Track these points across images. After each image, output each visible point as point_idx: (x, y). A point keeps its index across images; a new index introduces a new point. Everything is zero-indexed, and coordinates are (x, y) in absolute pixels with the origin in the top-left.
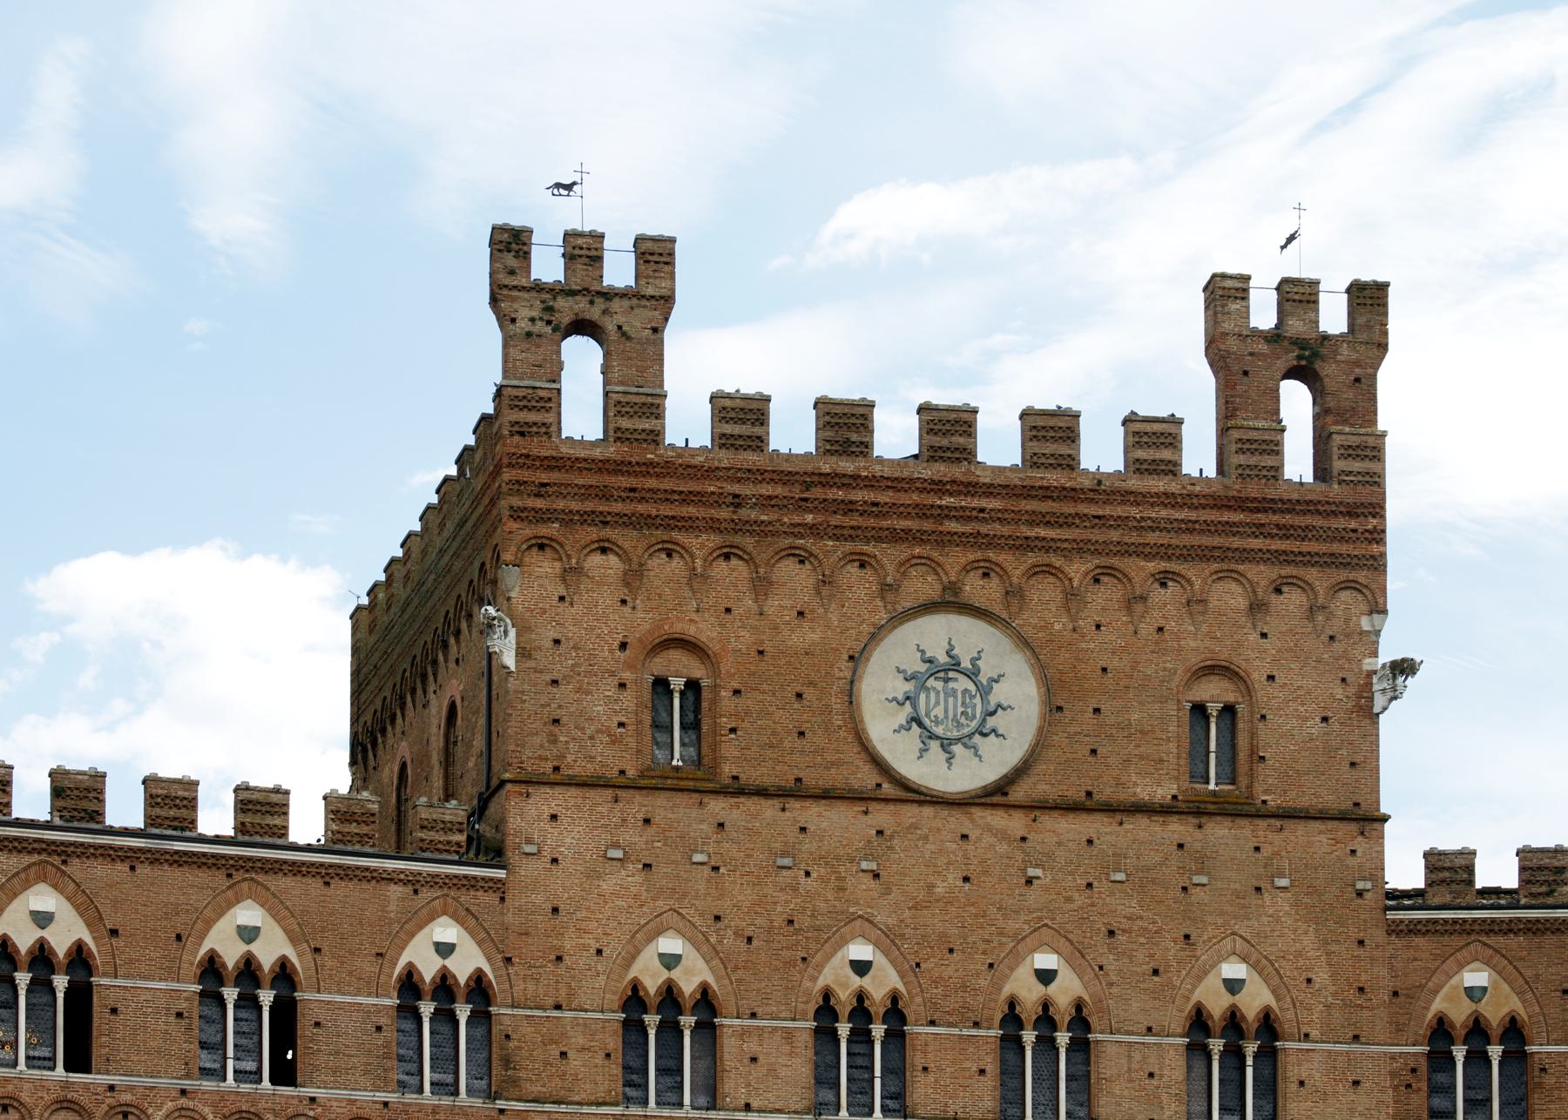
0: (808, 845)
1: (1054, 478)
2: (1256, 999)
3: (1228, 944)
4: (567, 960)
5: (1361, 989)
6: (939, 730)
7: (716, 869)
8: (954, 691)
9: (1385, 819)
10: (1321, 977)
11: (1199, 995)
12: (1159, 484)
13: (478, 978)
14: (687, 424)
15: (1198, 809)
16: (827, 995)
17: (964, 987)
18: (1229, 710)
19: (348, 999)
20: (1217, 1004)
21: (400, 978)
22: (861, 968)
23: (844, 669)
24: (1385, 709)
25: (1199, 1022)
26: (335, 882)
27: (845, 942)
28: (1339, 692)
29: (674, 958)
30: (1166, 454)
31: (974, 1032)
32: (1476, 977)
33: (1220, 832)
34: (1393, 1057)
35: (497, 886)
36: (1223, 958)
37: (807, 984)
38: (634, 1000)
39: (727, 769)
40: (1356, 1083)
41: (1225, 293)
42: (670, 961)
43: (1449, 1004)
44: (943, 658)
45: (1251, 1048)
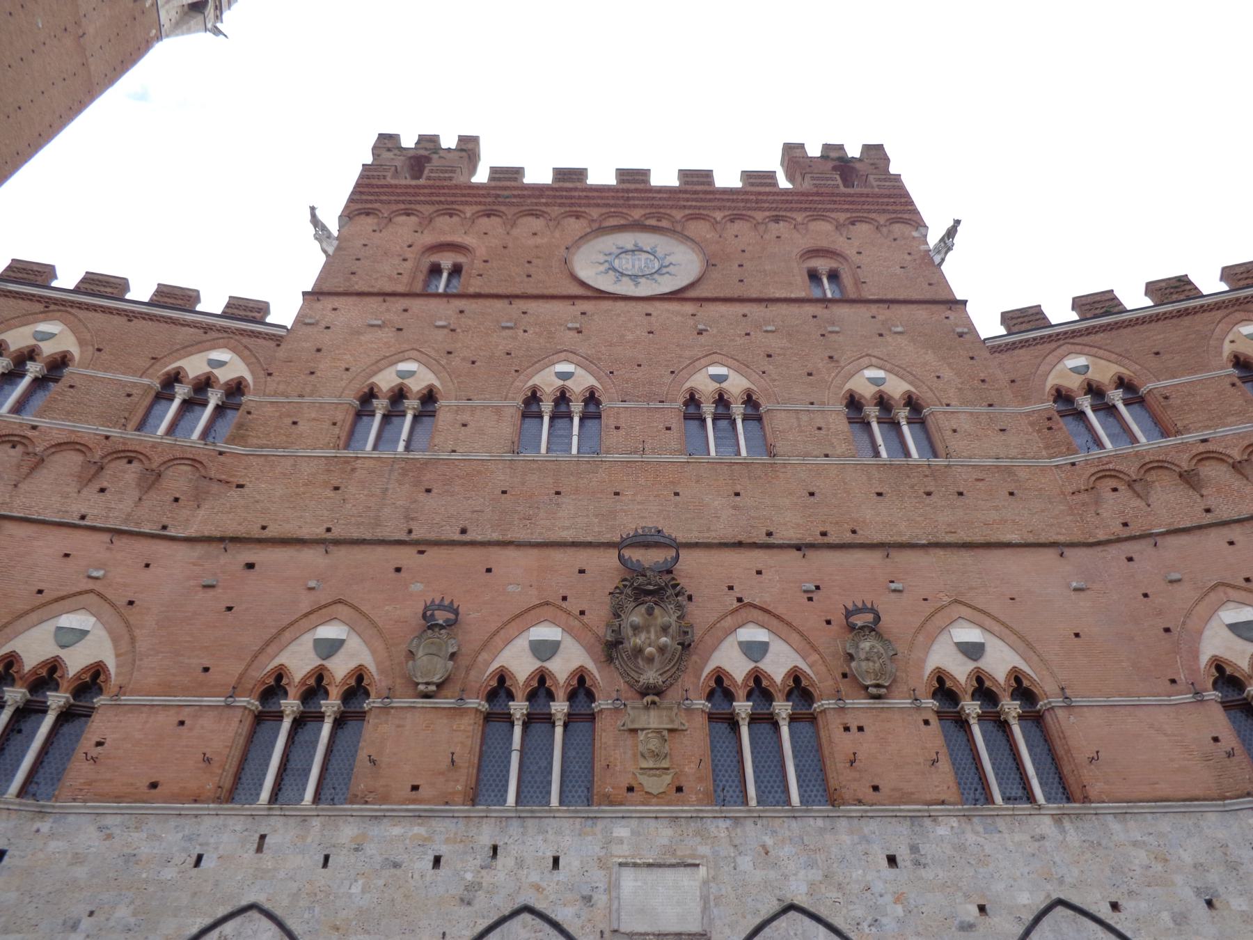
0: (526, 318)
3: (866, 360)
4: (318, 374)
5: (983, 381)
7: (453, 330)
9: (965, 302)
10: (947, 374)
17: (651, 383)
19: (109, 375)
21: (168, 374)
23: (563, 251)
24: (943, 260)
26: (135, 321)
28: (909, 258)
31: (661, 405)
34: (1028, 414)
35: (277, 340)
37: (517, 383)
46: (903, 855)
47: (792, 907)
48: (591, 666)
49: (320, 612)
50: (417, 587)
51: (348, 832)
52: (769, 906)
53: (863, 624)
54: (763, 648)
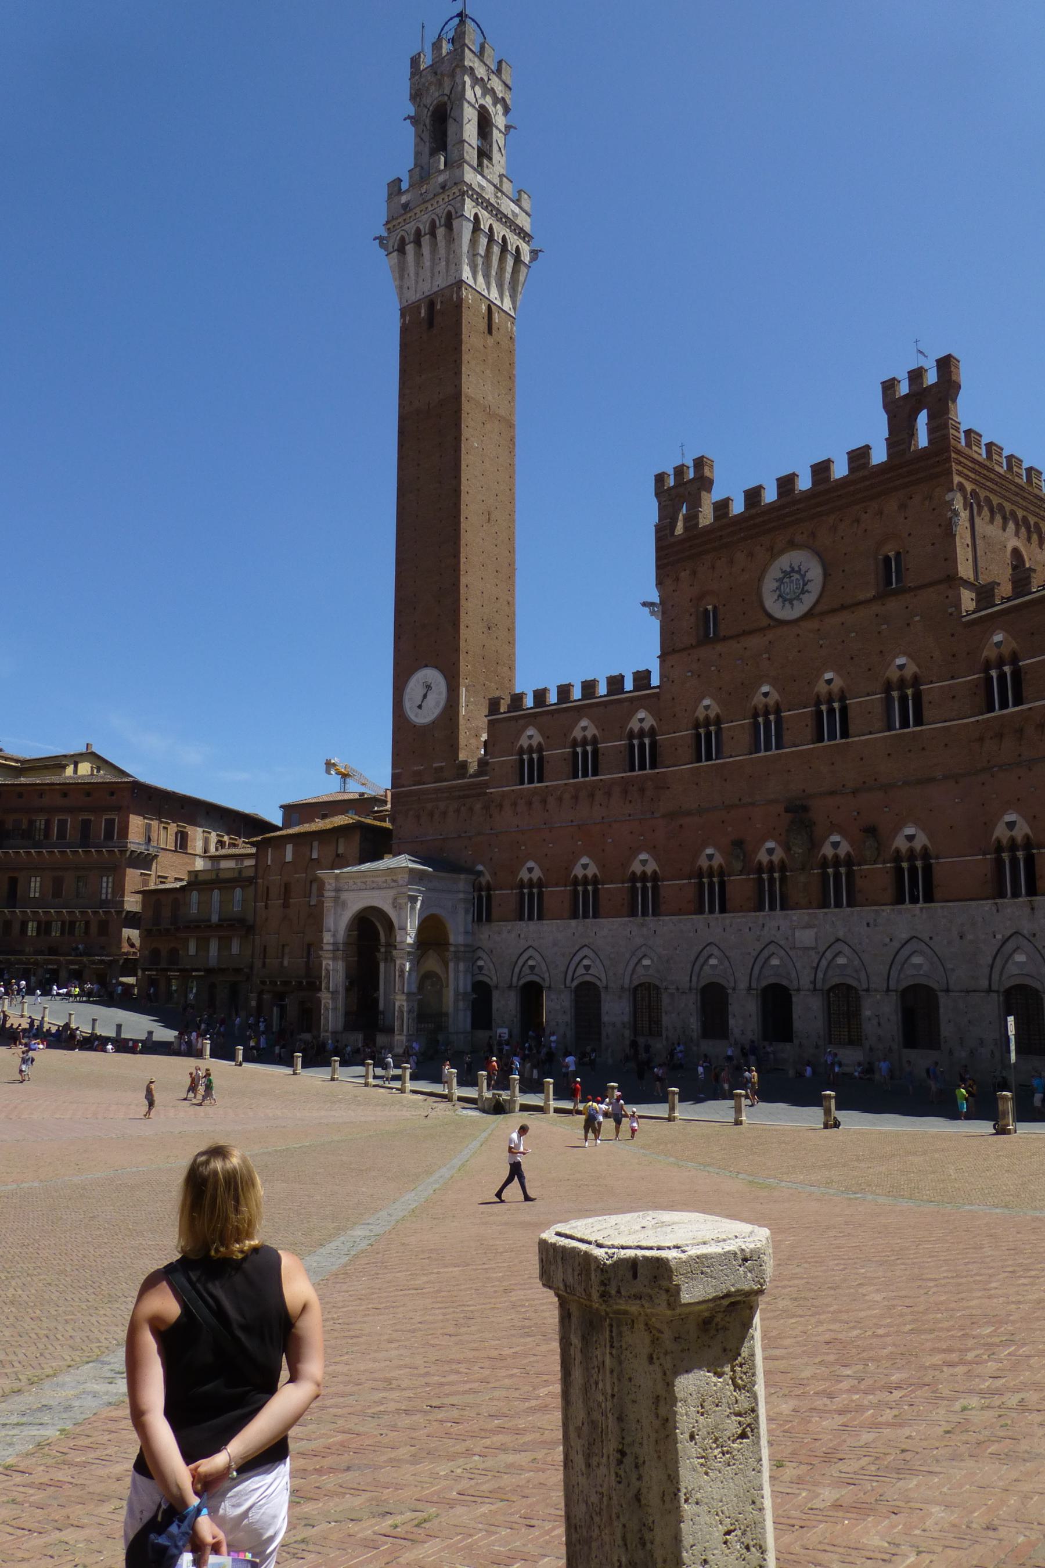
1: (821, 488)
2: (912, 669)
5: (954, 656)
6: (788, 597)
8: (792, 582)
11: (887, 674)
12: (860, 474)
13: (652, 728)
14: (706, 517)
15: (881, 597)
16: (755, 708)
18: (898, 554)
20: (894, 675)
22: (765, 695)
25: (888, 687)
27: (760, 686)
29: (708, 705)
30: (862, 461)
32: (998, 638)
33: (893, 605)
36: (895, 657)
38: (697, 726)
39: (722, 634)
40: (954, 697)
41: (889, 386)
42: (707, 708)
43: (989, 653)
44: (788, 569)
45: (909, 692)
46: (872, 922)
47: (838, 940)
48: (784, 856)
49: (705, 846)
50: (730, 829)
51: (728, 922)
52: (832, 940)
53: (871, 831)
54: (839, 843)
